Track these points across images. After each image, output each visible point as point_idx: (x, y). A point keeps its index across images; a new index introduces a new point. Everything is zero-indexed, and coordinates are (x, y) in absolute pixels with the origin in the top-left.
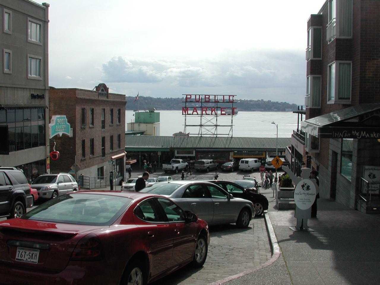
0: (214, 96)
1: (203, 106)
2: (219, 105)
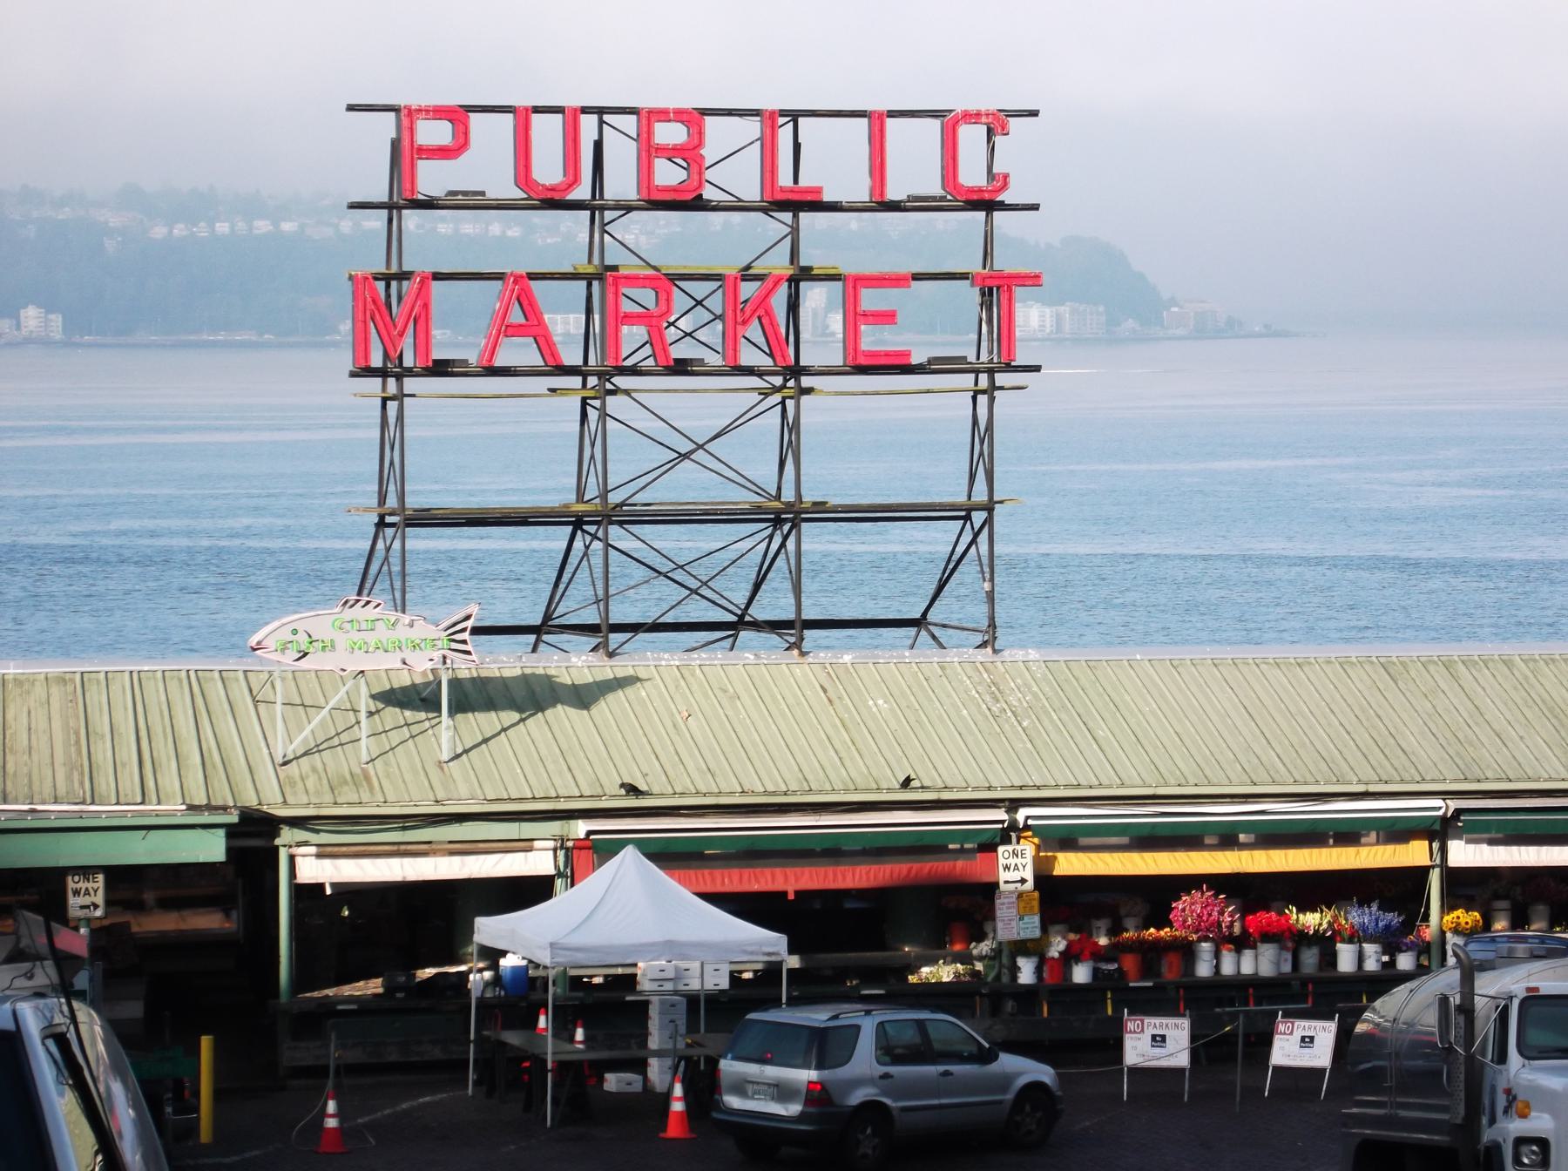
0: (753, 127)
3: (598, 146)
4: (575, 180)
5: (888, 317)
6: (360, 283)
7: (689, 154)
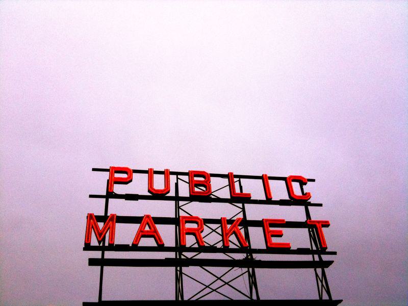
0: (225, 181)
1: (182, 214)
2: (254, 212)
3: (177, 185)
5: (280, 235)
6: (90, 217)
7: (207, 184)
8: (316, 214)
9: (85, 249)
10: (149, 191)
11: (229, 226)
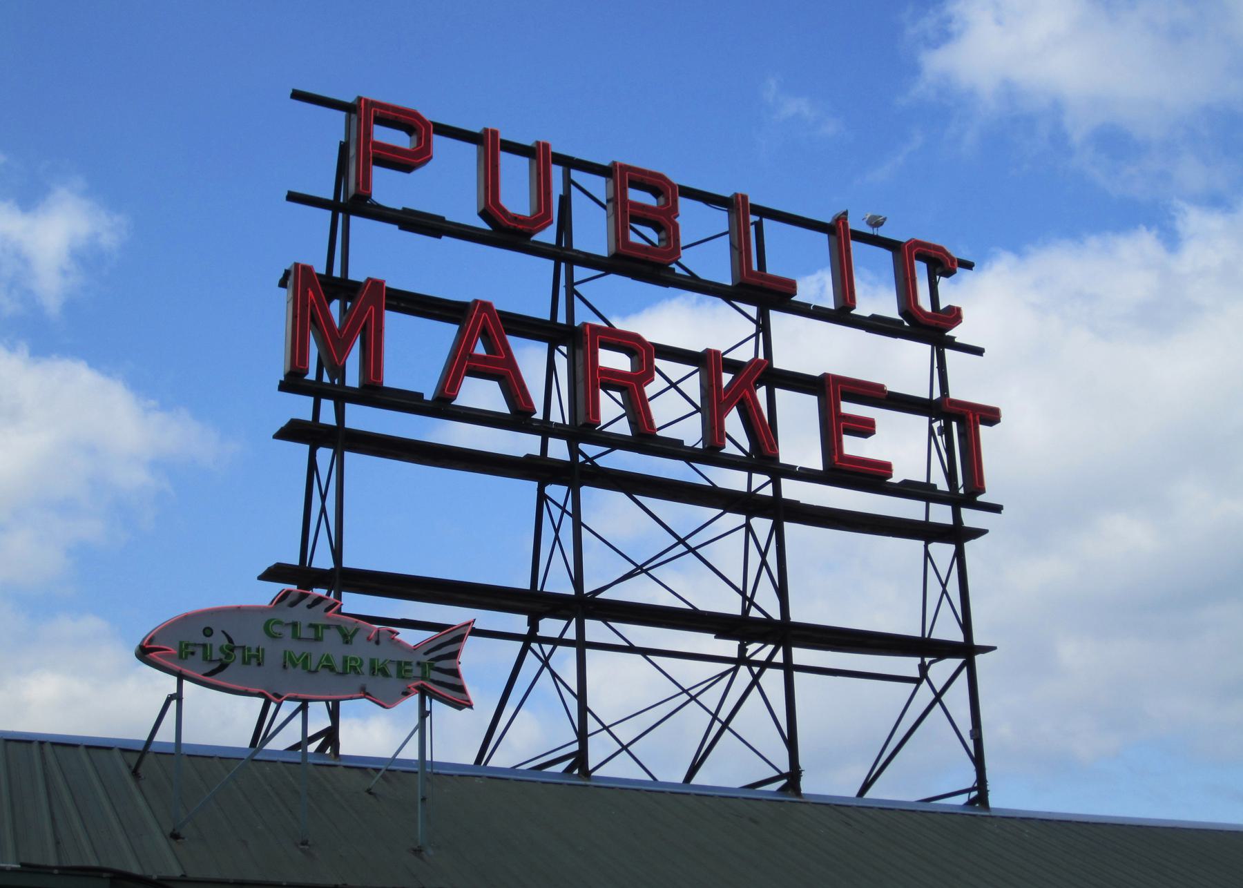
3: (565, 201)
4: (541, 220)
5: (865, 428)
7: (664, 221)
8: (968, 382)
9: (284, 387)
10: (484, 214)
11: (727, 378)
